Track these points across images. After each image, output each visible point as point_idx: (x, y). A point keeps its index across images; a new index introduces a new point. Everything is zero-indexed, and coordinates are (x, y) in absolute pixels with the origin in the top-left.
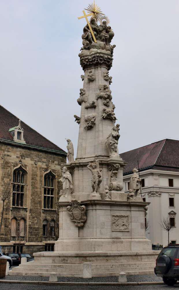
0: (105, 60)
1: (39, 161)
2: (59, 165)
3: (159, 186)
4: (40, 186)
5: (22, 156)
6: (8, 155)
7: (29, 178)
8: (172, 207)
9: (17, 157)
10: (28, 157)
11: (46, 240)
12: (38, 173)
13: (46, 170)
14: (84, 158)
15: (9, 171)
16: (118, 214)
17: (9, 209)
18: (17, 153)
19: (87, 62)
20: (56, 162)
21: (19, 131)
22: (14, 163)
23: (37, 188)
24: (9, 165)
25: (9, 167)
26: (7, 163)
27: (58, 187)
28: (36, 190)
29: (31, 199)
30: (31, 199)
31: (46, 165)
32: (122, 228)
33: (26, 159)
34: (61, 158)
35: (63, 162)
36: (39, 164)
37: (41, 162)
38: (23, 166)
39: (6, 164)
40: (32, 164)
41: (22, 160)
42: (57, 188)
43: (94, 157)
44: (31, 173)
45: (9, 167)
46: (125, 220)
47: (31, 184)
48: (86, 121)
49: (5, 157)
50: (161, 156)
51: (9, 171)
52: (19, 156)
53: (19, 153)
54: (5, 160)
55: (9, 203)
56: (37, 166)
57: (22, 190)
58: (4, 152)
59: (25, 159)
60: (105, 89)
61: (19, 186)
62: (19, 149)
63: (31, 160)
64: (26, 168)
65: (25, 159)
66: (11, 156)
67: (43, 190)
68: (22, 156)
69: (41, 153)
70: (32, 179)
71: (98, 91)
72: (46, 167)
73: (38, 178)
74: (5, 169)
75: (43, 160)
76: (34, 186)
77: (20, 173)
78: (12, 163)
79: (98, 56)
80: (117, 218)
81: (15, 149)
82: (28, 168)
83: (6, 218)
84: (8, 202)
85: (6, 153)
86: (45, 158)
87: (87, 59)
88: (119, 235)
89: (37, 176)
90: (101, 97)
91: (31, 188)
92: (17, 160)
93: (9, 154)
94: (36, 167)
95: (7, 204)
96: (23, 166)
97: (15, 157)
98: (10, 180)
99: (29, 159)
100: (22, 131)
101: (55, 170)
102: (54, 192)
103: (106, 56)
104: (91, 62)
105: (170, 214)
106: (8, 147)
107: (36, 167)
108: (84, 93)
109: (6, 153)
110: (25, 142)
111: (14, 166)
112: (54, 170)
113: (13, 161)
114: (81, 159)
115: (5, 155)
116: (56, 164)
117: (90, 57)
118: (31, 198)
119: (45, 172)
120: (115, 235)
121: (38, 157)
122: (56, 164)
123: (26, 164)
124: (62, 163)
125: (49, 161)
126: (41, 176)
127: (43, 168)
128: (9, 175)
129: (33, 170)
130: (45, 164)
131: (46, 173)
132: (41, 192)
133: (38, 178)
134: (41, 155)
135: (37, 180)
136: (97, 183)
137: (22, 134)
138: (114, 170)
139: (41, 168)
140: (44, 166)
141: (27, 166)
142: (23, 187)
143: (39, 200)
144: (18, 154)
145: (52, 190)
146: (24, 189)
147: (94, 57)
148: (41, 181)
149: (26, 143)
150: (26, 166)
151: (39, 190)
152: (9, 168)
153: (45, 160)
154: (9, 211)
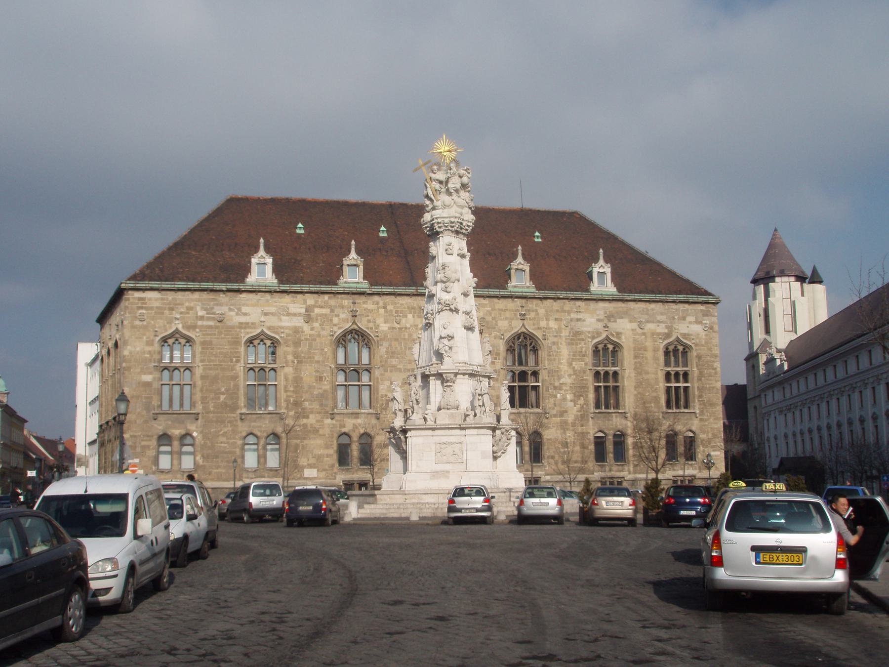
1: (648, 322)
2: (698, 322)
4: (656, 370)
5: (610, 317)
6: (578, 320)
7: (627, 357)
9: (599, 320)
10: (622, 318)
11: (674, 470)
12: (649, 344)
13: (668, 335)
15: (582, 348)
16: (445, 441)
17: (588, 416)
18: (598, 312)
20: (691, 319)
21: (602, 270)
22: (593, 332)
23: (647, 373)
24: (583, 337)
25: (583, 340)
26: (577, 334)
27: (697, 366)
28: (646, 377)
29: (635, 395)
30: (635, 395)
31: (667, 327)
32: (452, 459)
33: (618, 320)
34: (702, 307)
35: (707, 315)
36: (650, 327)
37: (653, 322)
38: (613, 335)
39: (576, 336)
40: (633, 330)
41: (609, 324)
42: (695, 369)
44: (632, 345)
45: (583, 340)
46: (457, 448)
47: (633, 367)
49: (573, 324)
51: (582, 348)
52: (602, 317)
53: (602, 312)
54: (572, 329)
55: (587, 405)
56: (645, 331)
57: (616, 380)
58: (569, 314)
59: (615, 321)
61: (607, 373)
62: (601, 304)
63: (631, 321)
64: (619, 338)
65: (615, 321)
66: (584, 321)
67: (661, 376)
68: (610, 317)
69: (653, 306)
70: (636, 357)
72: (666, 331)
73: (649, 355)
74: (573, 344)
75: (659, 318)
76: (639, 369)
77: (607, 351)
78: (589, 332)
80: (444, 446)
81: (592, 305)
82: (623, 337)
83: (583, 433)
84: (585, 404)
85: (573, 316)
86: (662, 314)
88: (448, 467)
89: (646, 350)
91: (633, 375)
92: (600, 326)
93: (579, 316)
94: (644, 334)
95: (582, 407)
96: (613, 335)
97: (593, 320)
98: (586, 364)
99: (626, 320)
100: (608, 269)
101: (688, 335)
102: (690, 377)
103: (446, 220)
106: (578, 303)
107: (644, 334)
109: (573, 316)
110: (615, 289)
111: (593, 338)
112: (685, 335)
113: (590, 329)
115: (571, 320)
116: (690, 323)
118: (636, 392)
119: (664, 340)
120: (440, 467)
121: (647, 314)
122: (690, 323)
123: (620, 330)
124: (706, 318)
125: (674, 318)
126: (656, 350)
127: (659, 334)
128: (584, 356)
129: (635, 340)
130: (663, 325)
131: (666, 342)
132: (657, 379)
133: (649, 355)
134: (653, 309)
135: (646, 358)
137: (609, 276)
139: (653, 334)
140: (662, 329)
141: (621, 333)
142: (615, 374)
143: (654, 394)
144: (601, 314)
145: (686, 375)
146: (620, 377)
148: (656, 359)
149: (619, 291)
150: (619, 334)
151: (651, 376)
152: (583, 343)
153: (663, 318)
154: (588, 420)
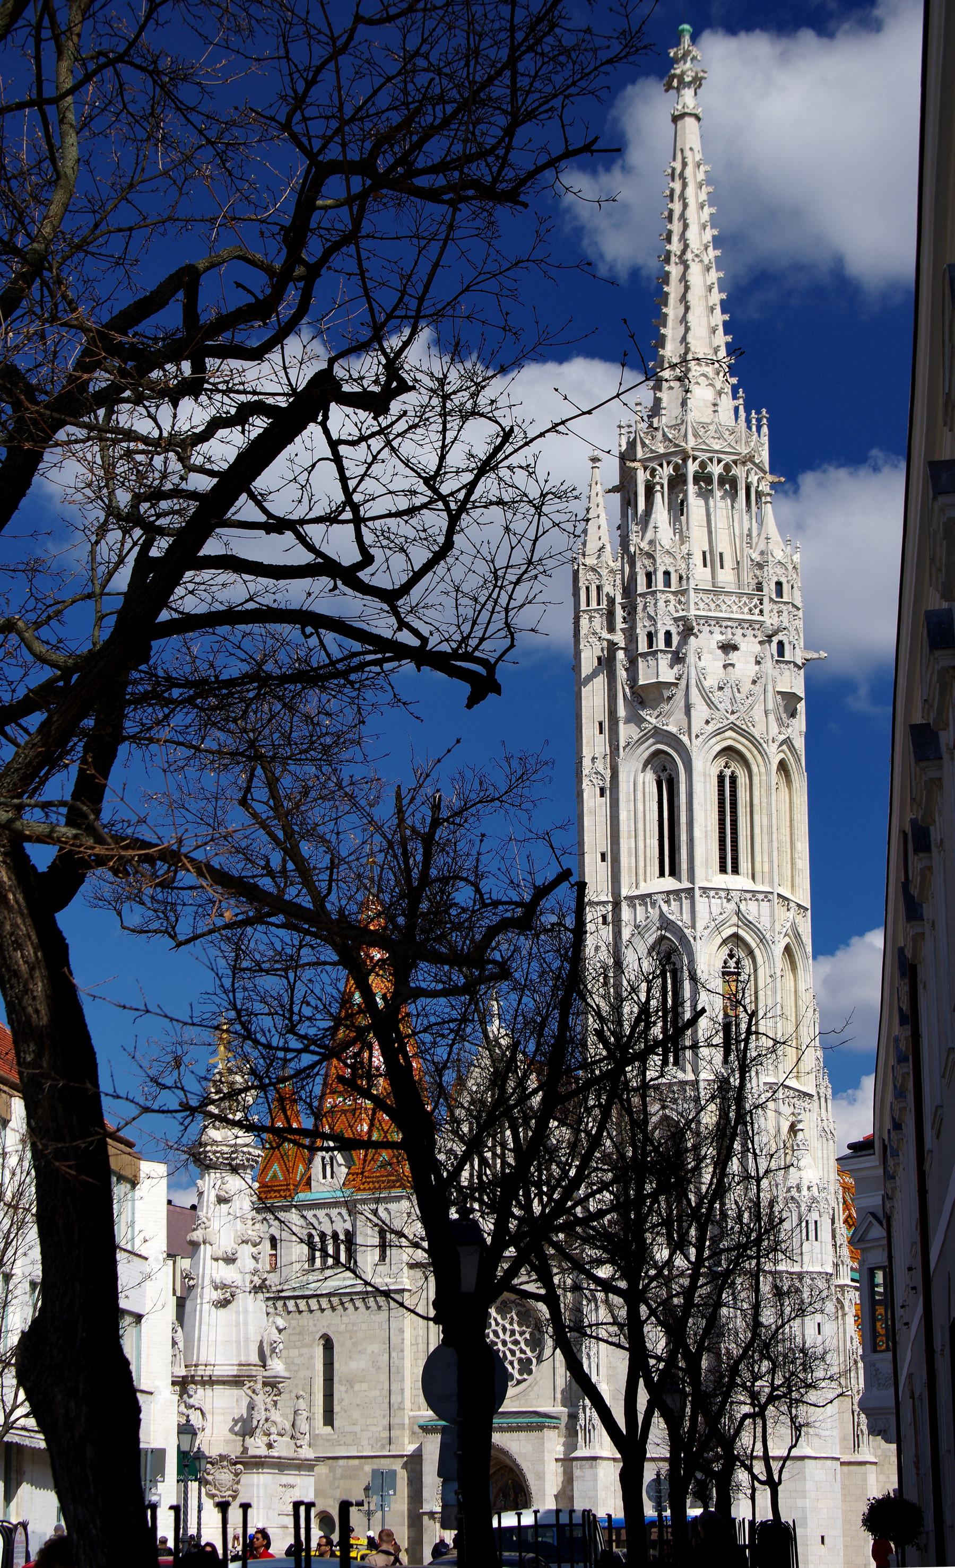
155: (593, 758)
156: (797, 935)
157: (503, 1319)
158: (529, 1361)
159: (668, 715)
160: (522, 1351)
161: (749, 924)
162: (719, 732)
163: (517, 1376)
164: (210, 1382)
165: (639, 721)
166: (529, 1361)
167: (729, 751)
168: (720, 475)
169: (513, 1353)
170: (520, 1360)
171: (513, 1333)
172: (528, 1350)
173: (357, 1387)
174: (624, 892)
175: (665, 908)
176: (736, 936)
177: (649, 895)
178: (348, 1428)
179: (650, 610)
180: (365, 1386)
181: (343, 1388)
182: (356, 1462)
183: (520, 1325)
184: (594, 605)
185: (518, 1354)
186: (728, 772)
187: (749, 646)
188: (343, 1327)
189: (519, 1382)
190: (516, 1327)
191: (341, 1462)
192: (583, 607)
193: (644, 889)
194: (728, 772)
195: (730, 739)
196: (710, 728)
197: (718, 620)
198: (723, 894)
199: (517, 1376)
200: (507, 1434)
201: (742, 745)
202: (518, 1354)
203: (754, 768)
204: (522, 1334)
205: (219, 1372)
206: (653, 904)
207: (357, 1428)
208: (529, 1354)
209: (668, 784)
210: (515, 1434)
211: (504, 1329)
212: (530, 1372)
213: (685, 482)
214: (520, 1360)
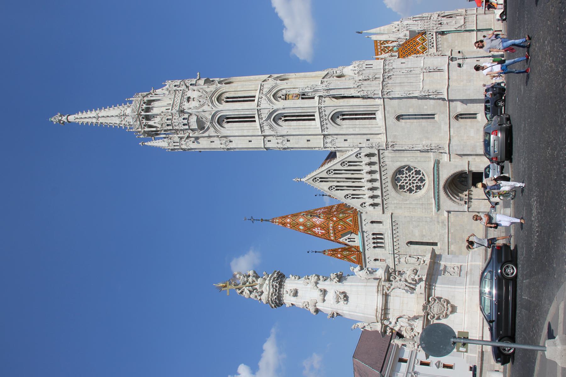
0: (279, 277)
3: (406, 373)
8: (431, 364)
14: (377, 307)
19: (275, 295)
43: (378, 295)
48: (338, 302)
50: (371, 365)
60: (309, 279)
71: (309, 286)
79: (273, 281)
87: (272, 294)
90: (316, 283)
104: (276, 290)
105: (438, 367)
108: (306, 303)
114: (377, 311)
117: (271, 290)
136: (407, 284)
138: (395, 274)
147: (273, 286)
155: (221, 144)
156: (277, 77)
157: (401, 180)
158: (416, 171)
159: (206, 118)
160: (413, 174)
161: (270, 91)
162: (212, 102)
163: (421, 176)
164: (386, 309)
165: (208, 128)
166: (416, 171)
167: (219, 99)
168: (146, 105)
169: (413, 177)
170: (416, 174)
171: (406, 177)
172: (412, 172)
173: (424, 233)
174: (260, 133)
175: (264, 119)
176: (273, 96)
177: (260, 125)
178: (438, 237)
179: (177, 124)
180: (424, 231)
181: (425, 239)
182: (450, 235)
183: (403, 174)
184: (178, 144)
185: (414, 175)
186: (225, 100)
187: (189, 94)
188: (404, 238)
189: (423, 175)
190: (404, 176)
191: (450, 240)
192: (179, 147)
193: (259, 127)
194: (225, 100)
195: (214, 99)
196: (210, 105)
197: (181, 103)
198: (260, 100)
199: (421, 176)
200: (440, 179)
201: (217, 95)
202: (414, 175)
203: (224, 91)
204: (406, 174)
205: (380, 306)
206: (263, 123)
207: (438, 234)
208: (414, 171)
209: (230, 119)
210: (440, 176)
211: (405, 180)
212: (420, 171)
213: (148, 115)
214: (416, 174)
